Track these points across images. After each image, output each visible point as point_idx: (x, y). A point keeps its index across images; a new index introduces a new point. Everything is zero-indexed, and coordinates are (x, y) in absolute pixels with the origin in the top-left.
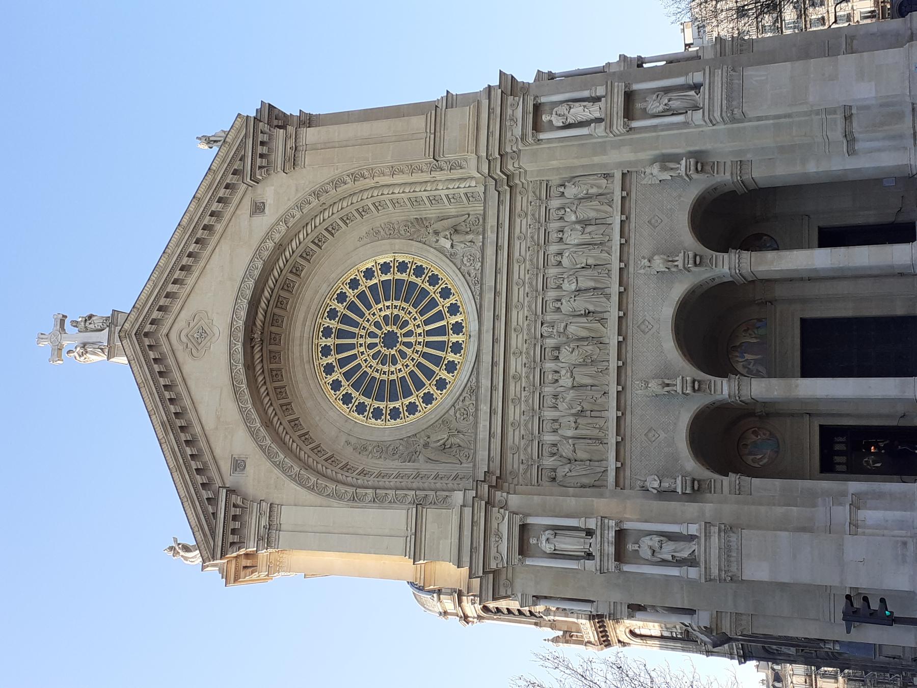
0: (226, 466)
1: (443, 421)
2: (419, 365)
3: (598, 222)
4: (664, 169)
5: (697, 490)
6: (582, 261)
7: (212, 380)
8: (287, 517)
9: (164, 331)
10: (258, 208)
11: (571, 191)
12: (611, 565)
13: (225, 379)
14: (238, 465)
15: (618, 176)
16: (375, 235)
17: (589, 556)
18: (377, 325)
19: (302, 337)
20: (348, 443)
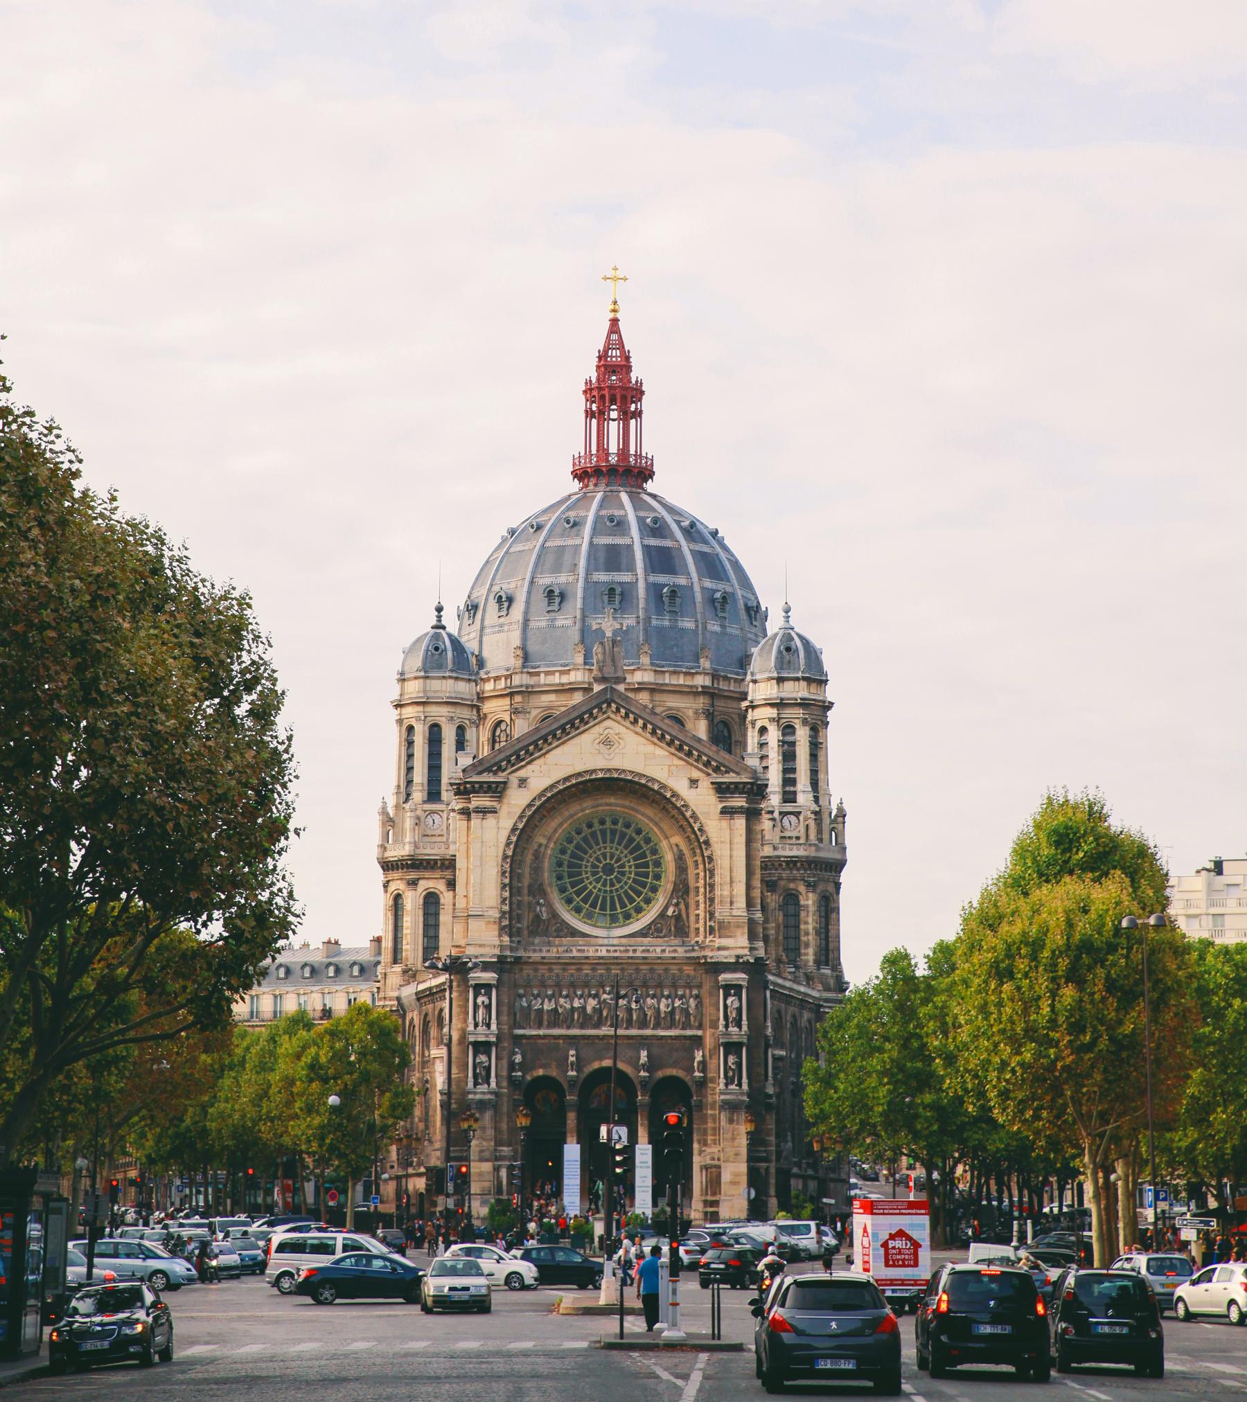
0: (522, 773)
1: (555, 915)
2: (591, 893)
3: (673, 1020)
4: (699, 1063)
5: (512, 1082)
6: (649, 1013)
7: (577, 756)
8: (491, 820)
9: (613, 716)
10: (694, 782)
11: (692, 1002)
12: (472, 1039)
13: (580, 768)
14: (523, 782)
15: (700, 1033)
16: (680, 858)
17: (476, 1025)
18: (618, 860)
19: (610, 805)
20: (540, 845)
